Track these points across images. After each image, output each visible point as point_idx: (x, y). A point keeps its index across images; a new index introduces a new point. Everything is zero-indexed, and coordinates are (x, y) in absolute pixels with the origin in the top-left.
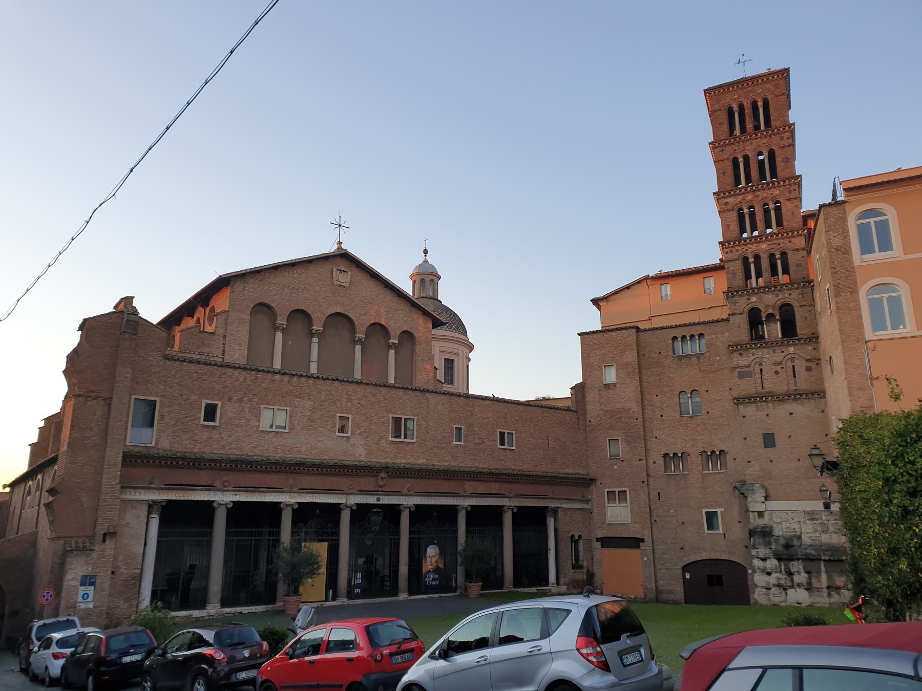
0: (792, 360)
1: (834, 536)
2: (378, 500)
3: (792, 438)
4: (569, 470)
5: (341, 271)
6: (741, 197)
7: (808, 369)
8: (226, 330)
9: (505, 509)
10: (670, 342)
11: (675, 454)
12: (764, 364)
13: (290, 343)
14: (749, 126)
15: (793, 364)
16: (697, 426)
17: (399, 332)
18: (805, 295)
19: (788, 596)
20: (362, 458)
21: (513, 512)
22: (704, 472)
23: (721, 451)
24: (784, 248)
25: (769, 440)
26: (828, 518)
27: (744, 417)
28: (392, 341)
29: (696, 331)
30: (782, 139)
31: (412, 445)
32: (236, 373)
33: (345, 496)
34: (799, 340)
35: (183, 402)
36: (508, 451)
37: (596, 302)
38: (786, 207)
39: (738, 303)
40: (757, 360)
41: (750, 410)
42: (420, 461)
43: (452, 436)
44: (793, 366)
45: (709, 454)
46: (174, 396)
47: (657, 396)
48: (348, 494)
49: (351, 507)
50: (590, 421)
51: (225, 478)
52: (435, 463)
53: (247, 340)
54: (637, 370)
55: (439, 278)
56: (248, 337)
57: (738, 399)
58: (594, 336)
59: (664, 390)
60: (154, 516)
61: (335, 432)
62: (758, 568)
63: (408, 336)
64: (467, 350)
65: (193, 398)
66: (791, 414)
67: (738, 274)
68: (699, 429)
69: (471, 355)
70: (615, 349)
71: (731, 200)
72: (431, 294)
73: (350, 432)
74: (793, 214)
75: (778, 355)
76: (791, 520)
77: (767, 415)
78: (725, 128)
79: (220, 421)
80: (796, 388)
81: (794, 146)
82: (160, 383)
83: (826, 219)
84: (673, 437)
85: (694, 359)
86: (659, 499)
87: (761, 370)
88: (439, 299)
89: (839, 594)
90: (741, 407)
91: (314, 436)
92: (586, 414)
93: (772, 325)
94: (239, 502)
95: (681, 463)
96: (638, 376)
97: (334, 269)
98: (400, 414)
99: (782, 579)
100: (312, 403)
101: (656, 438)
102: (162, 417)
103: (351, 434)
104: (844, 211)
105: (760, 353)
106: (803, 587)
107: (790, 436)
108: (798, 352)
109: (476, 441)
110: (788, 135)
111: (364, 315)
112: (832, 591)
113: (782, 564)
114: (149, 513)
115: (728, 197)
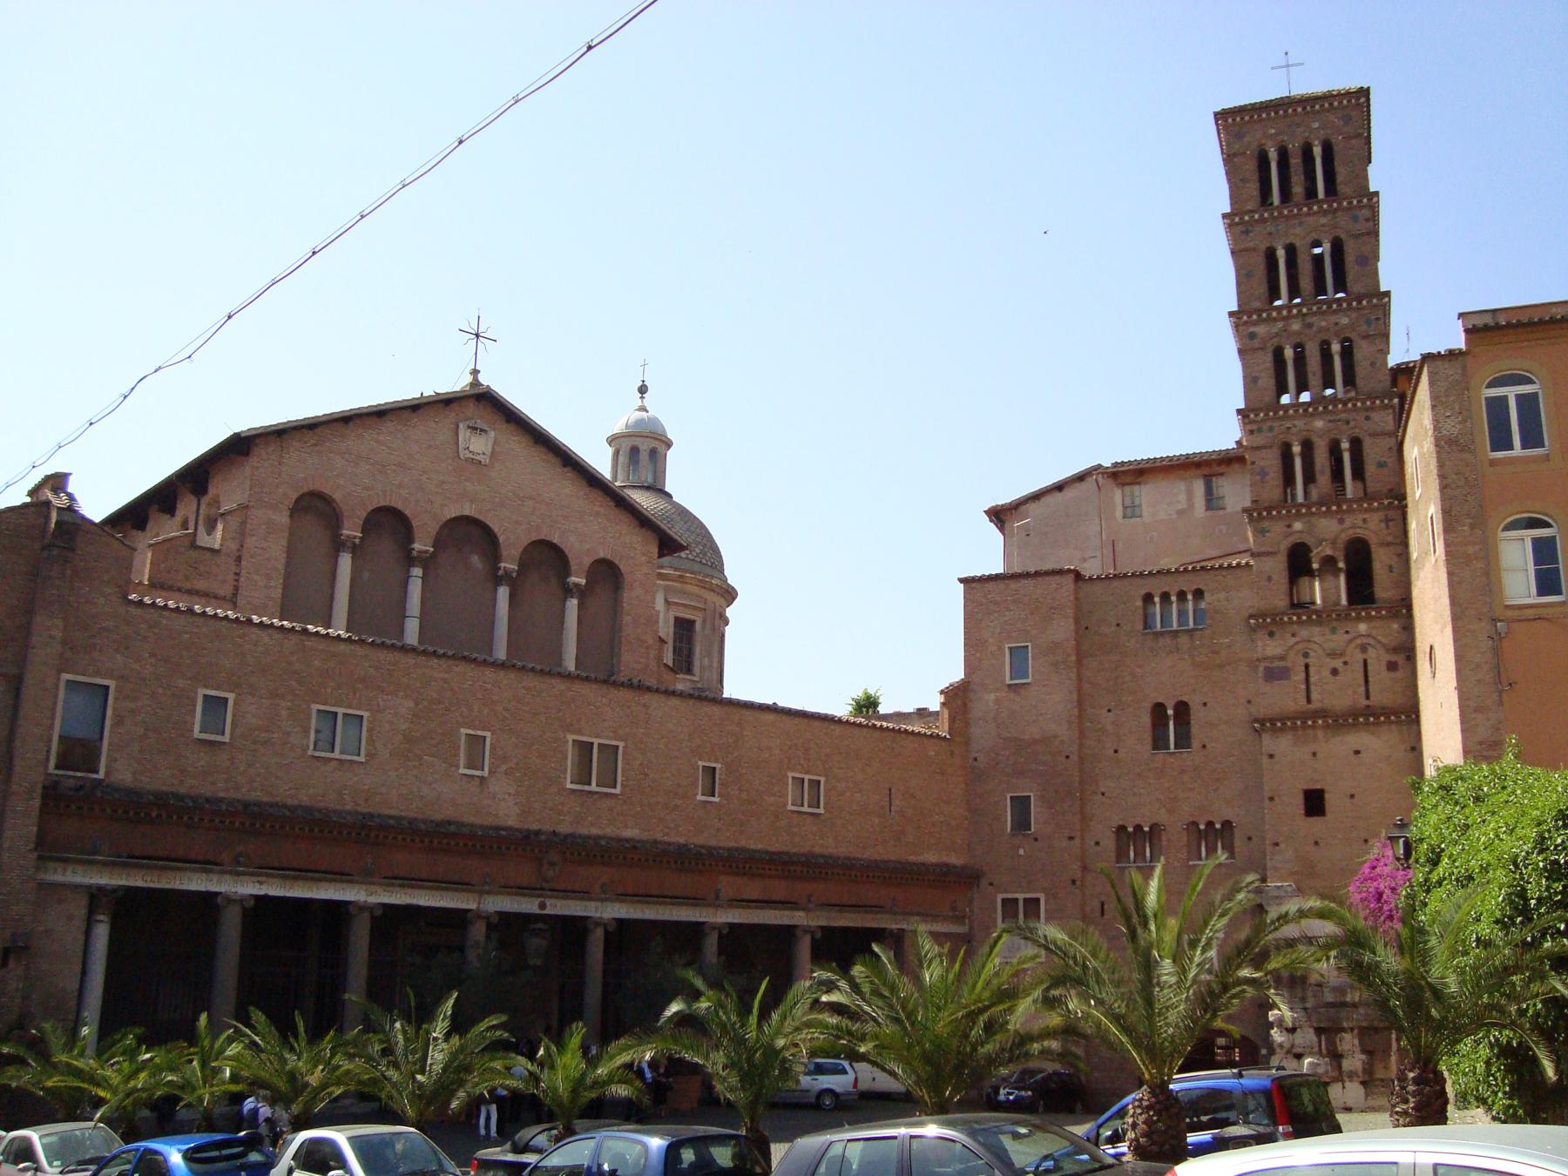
0: (1364, 648)
2: (543, 906)
3: (1355, 800)
4: (931, 857)
5: (476, 429)
6: (1280, 324)
7: (1392, 666)
8: (242, 546)
9: (798, 932)
10: (1139, 603)
11: (1138, 828)
12: (1312, 654)
13: (366, 575)
14: (1298, 189)
15: (1365, 656)
16: (1183, 772)
17: (588, 561)
18: (1390, 524)
20: (512, 822)
21: (813, 939)
22: (1191, 863)
23: (1227, 824)
24: (1357, 430)
25: (1314, 803)
27: (1271, 756)
28: (573, 579)
29: (1189, 585)
30: (1355, 219)
31: (614, 801)
32: (264, 636)
33: (476, 896)
34: (1378, 610)
35: (160, 691)
36: (809, 819)
37: (998, 516)
38: (1362, 351)
39: (1268, 531)
40: (1300, 646)
41: (1281, 744)
42: (628, 833)
43: (694, 784)
44: (1365, 662)
45: (1202, 827)
46: (144, 679)
47: (1109, 711)
48: (482, 893)
49: (488, 918)
50: (976, 759)
51: (239, 848)
52: (659, 837)
53: (281, 565)
54: (1073, 658)
55: (669, 444)
56: (283, 561)
57: (1262, 722)
58: (990, 586)
59: (1124, 699)
60: (101, 917)
61: (457, 766)
62: (1281, 1046)
63: (607, 573)
64: (721, 601)
65: (181, 683)
66: (1357, 752)
67: (1272, 475)
68: (1185, 778)
69: (730, 612)
70: (1032, 613)
71: (1261, 330)
72: (650, 480)
73: (486, 769)
74: (1373, 364)
75: (1338, 640)
77: (1314, 754)
78: (1253, 188)
79: (232, 734)
80: (1367, 702)
81: (1376, 234)
82: (117, 650)
83: (1432, 383)
84: (1135, 794)
85: (1184, 640)
86: (1103, 913)
87: (1307, 666)
88: (666, 490)
90: (1266, 738)
91: (415, 772)
92: (967, 743)
93: (1330, 579)
94: (266, 897)
95: (1148, 845)
96: (1075, 670)
97: (461, 426)
98: (589, 736)
100: (412, 704)
101: (1103, 794)
102: (119, 721)
103: (489, 773)
104: (1464, 368)
105: (1304, 633)
106: (1355, 1079)
107: (1352, 796)
108: (1374, 632)
109: (744, 796)
110: (1366, 213)
111: (517, 522)
113: (1323, 1038)
114: (91, 912)
115: (1256, 323)
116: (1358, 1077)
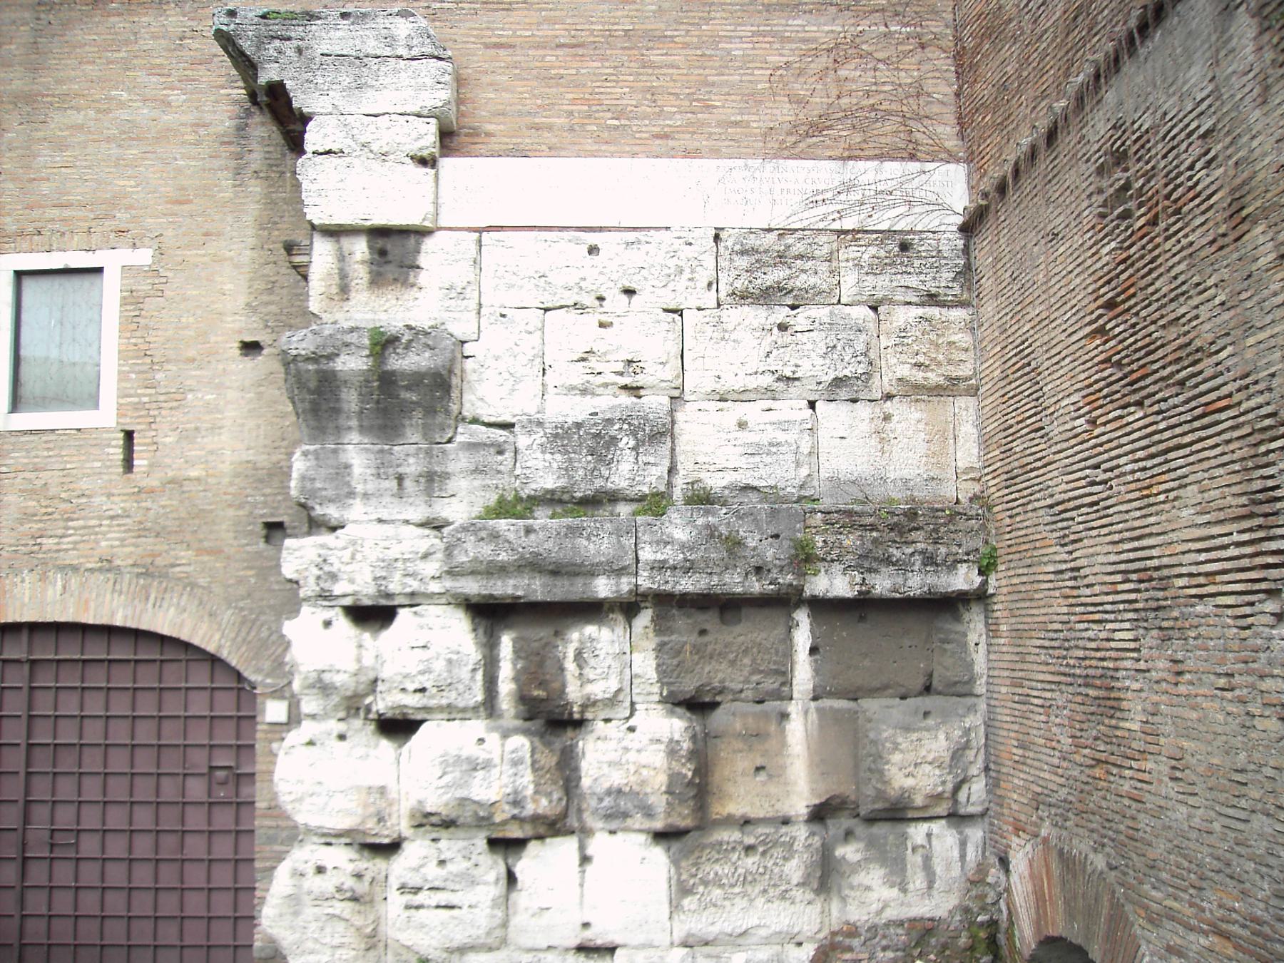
1: (906, 416)
19: (521, 899)
26: (881, 284)
62: (322, 687)
76: (617, 301)
89: (897, 874)
99: (487, 765)
106: (638, 821)
112: (848, 835)
116: (649, 813)
